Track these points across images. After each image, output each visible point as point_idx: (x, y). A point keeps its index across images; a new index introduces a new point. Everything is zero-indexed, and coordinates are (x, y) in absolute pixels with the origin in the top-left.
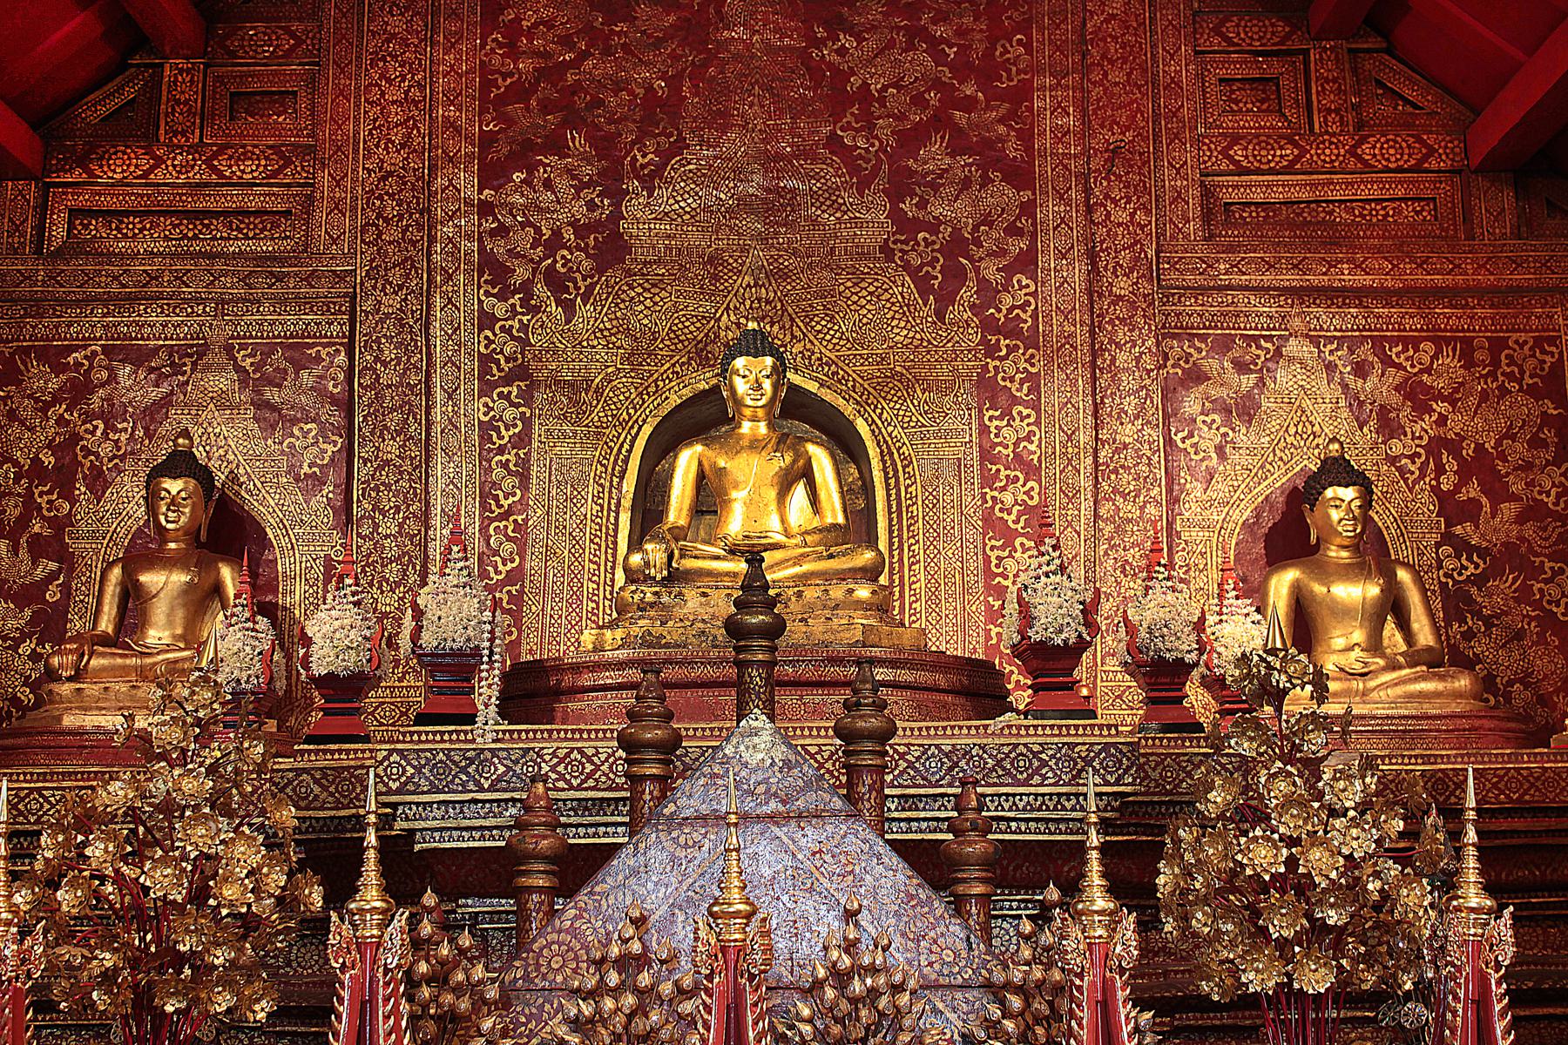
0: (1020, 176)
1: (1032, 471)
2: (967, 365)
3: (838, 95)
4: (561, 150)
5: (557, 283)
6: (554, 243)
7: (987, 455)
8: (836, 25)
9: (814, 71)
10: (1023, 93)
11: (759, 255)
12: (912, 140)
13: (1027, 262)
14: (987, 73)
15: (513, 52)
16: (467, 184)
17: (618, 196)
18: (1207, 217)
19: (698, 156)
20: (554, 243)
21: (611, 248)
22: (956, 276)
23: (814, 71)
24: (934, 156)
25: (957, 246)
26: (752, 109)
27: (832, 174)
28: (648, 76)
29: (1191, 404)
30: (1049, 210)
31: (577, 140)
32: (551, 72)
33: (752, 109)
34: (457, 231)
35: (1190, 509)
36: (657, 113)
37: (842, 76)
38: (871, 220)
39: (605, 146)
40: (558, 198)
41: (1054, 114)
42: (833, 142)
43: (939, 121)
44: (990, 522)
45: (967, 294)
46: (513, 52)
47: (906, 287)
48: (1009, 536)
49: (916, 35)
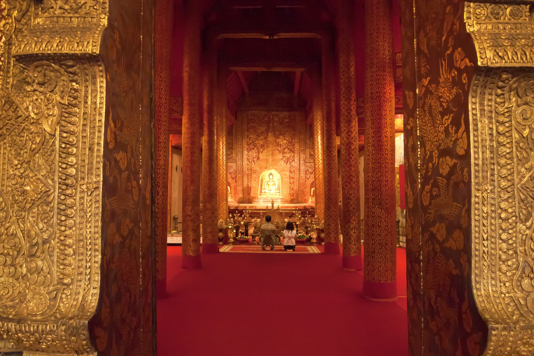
0: (294, 152)
1: (294, 178)
2: (288, 169)
3: (278, 144)
4: (253, 149)
5: (254, 161)
6: (254, 158)
7: (290, 177)
8: (278, 138)
9: (276, 142)
10: (294, 145)
11: (270, 160)
12: (285, 149)
13: (294, 160)
14: (291, 143)
15: (250, 140)
16: (246, 153)
17: (259, 154)
18: (310, 155)
19: (266, 151)
20: (254, 158)
21: (258, 158)
22: (288, 161)
23: (276, 142)
24: (286, 150)
25: (288, 158)
26: (271, 146)
27: (277, 152)
28: (261, 143)
29: (307, 173)
30: (296, 155)
31: (255, 149)
32: (253, 142)
33: (271, 146)
34: (245, 157)
35: (307, 182)
36: (262, 146)
37: (278, 143)
38: (280, 156)
39: (257, 148)
40: (254, 153)
41: (297, 147)
42: (278, 149)
43: (287, 147)
44: (290, 183)
45: (289, 163)
46: (250, 140)
47: (283, 162)
48: (291, 184)
49: (285, 139)
